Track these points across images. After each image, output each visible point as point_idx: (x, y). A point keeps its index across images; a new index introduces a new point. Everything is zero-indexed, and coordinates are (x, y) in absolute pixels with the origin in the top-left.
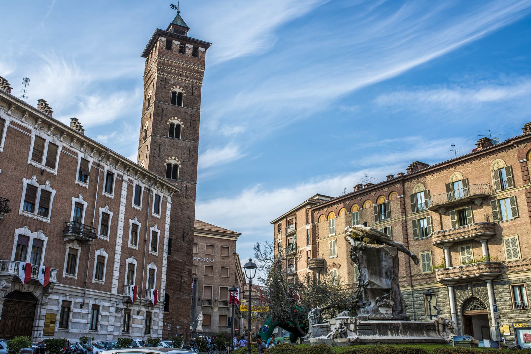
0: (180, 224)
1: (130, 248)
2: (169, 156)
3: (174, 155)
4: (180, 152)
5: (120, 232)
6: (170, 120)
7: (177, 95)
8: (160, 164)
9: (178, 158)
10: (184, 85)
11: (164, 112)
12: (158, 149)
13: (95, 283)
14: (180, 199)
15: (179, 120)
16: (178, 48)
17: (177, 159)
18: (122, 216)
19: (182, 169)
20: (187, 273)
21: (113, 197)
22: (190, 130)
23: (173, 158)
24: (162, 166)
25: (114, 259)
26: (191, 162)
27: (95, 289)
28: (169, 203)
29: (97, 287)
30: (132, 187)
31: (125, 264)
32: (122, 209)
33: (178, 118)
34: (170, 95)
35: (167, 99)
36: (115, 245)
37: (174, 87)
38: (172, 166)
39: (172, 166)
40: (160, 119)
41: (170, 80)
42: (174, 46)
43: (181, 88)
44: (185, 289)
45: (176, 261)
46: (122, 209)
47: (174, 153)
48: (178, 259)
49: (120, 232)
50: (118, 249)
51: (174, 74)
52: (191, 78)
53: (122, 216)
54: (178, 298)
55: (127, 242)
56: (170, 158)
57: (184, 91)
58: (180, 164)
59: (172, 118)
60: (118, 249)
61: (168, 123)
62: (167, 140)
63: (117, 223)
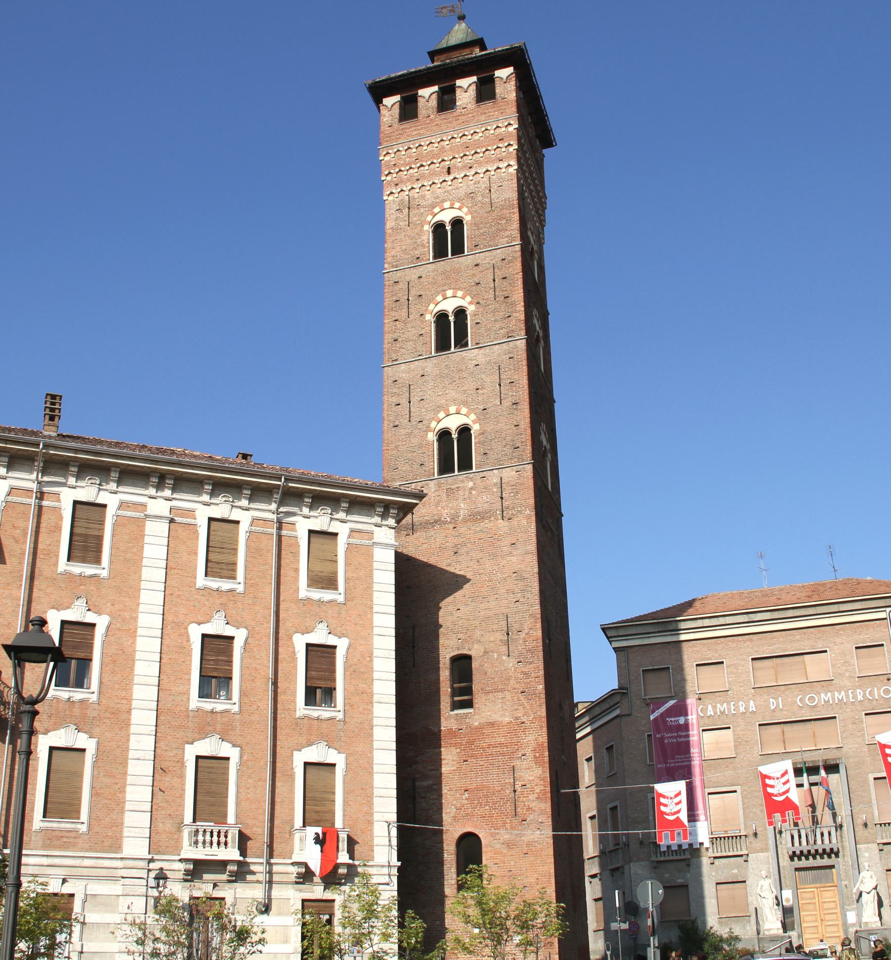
0: (492, 604)
1: (198, 710)
2: (438, 409)
3: (454, 401)
4: (470, 385)
5: (146, 669)
6: (432, 306)
7: (448, 228)
8: (415, 441)
9: (465, 403)
10: (462, 193)
11: (413, 292)
12: (404, 401)
13: (42, 830)
14: (487, 524)
15: (460, 293)
16: (434, 102)
17: (464, 410)
18: (149, 621)
19: (482, 433)
20: (530, 755)
21: (104, 573)
22: (494, 311)
23: (453, 409)
24: (420, 446)
25: (127, 749)
26: (507, 403)
27: (45, 847)
28: (387, 546)
29: (52, 840)
30: (192, 528)
31: (182, 763)
32: (151, 598)
33: (456, 289)
34: (428, 238)
35: (417, 253)
36: (129, 712)
37: (437, 210)
38: (455, 436)
39: (455, 436)
40: (403, 313)
41: (423, 197)
42: (421, 102)
43: (457, 205)
44: (529, 809)
45: (492, 724)
46: (151, 598)
47: (453, 394)
48: (496, 717)
49: (146, 669)
50: (143, 720)
51: (433, 174)
52: (480, 164)
53: (149, 621)
54: (509, 845)
55: (187, 693)
56: (442, 415)
57: (465, 210)
58: (474, 422)
59: (439, 298)
60: (143, 720)
61: (429, 317)
62: (430, 366)
63: (134, 643)
